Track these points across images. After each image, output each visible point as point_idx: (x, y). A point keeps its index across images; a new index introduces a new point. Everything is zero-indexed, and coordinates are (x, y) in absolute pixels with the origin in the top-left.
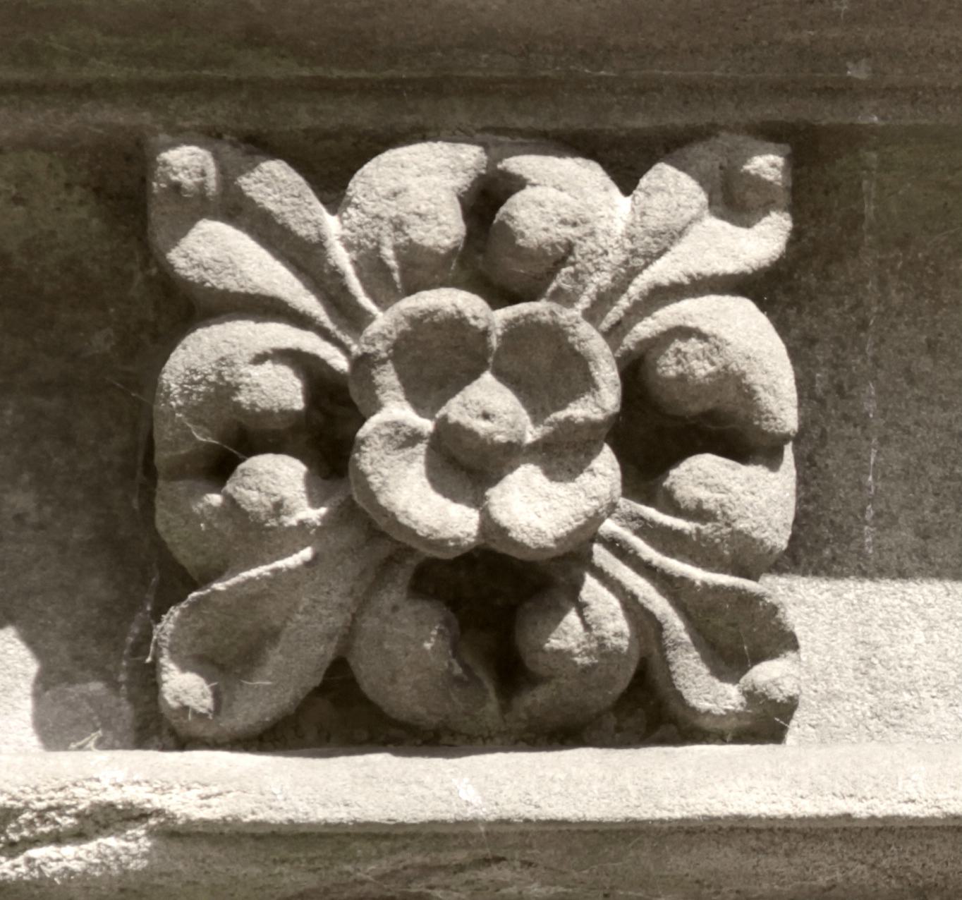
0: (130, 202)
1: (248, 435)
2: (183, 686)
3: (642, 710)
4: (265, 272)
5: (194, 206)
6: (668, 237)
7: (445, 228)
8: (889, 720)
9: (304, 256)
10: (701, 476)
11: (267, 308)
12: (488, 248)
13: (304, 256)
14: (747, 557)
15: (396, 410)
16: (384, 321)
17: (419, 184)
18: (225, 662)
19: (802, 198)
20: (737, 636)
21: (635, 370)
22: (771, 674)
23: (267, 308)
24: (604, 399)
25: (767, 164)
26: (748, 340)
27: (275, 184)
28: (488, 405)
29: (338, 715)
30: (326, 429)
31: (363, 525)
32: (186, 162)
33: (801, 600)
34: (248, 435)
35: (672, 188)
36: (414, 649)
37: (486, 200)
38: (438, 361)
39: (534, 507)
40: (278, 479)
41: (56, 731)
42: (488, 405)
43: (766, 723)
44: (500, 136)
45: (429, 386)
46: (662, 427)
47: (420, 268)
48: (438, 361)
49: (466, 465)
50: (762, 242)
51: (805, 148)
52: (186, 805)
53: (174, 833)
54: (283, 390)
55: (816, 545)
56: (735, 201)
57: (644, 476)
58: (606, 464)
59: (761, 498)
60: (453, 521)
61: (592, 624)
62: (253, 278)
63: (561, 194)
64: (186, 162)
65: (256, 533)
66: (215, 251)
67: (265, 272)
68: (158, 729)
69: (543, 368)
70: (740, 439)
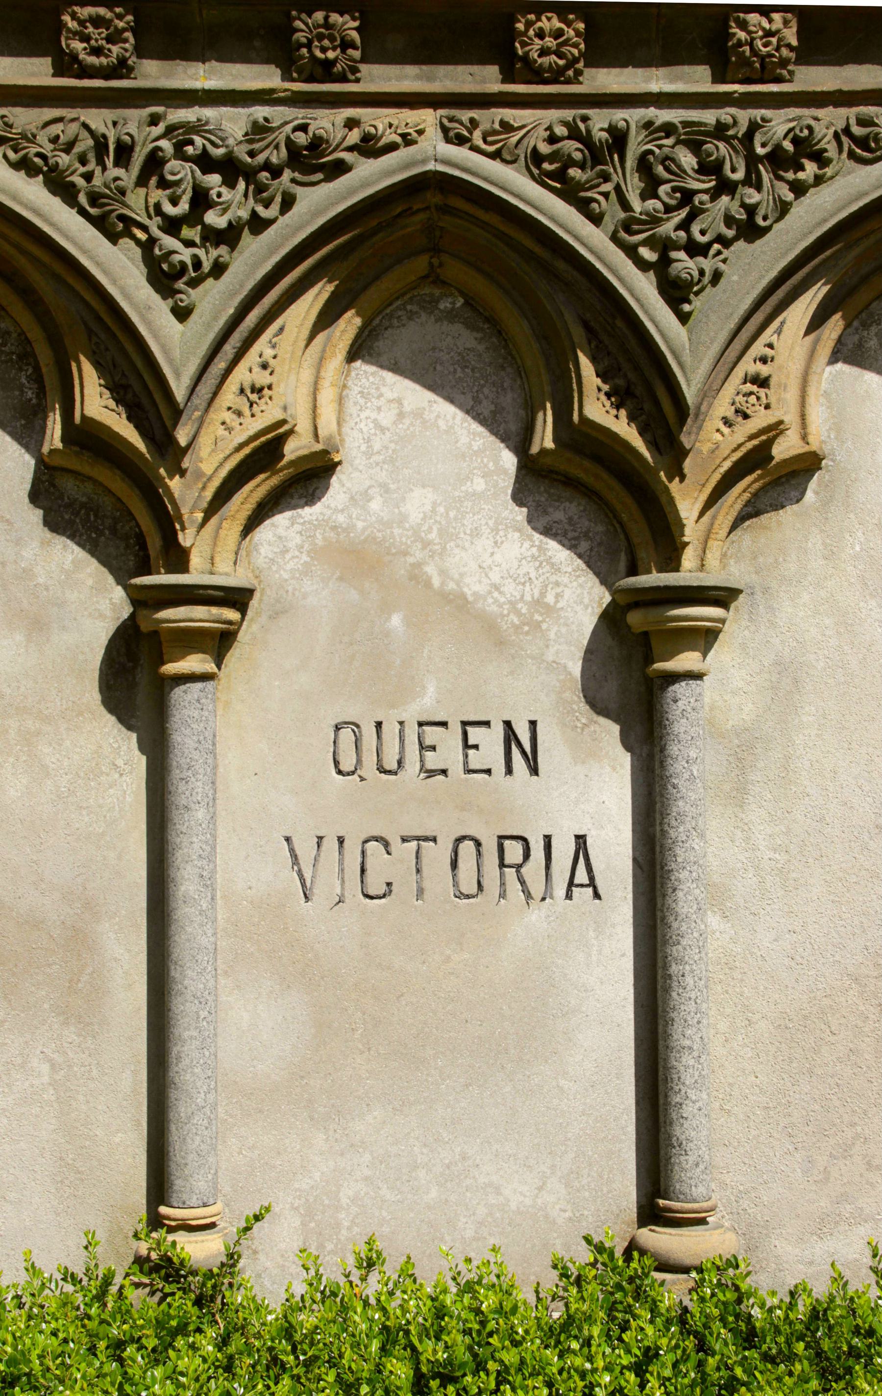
0: (291, 19)
1: (302, 45)
2: (295, 75)
3: (343, 79)
4: (303, 27)
5: (295, 19)
6: (346, 23)
7: (321, 21)
8: (372, 81)
9: (306, 24)
10: (350, 52)
11: (303, 31)
12: (327, 25)
13: (306, 24)
14: (355, 61)
15: (316, 43)
16: (315, 32)
17: (319, 16)
18: (299, 73)
19: (361, 18)
20: (355, 70)
21: (342, 39)
22: (358, 75)
23: (303, 31)
24: (338, 42)
25: (357, 14)
26: (355, 35)
27: (304, 16)
28: (326, 43)
29: (311, 79)
30: (309, 45)
31: (313, 56)
32: (294, 13)
33: (363, 67)
34: (302, 45)
35: (347, 17)
36: (319, 71)
37: (326, 18)
38: (320, 37)
39: (331, 55)
40: (304, 51)
41: (283, 80)
42: (326, 43)
43: (358, 81)
44: (328, 11)
45: (319, 42)
46: (346, 44)
47: (319, 26)
48: (320, 37)
49: (324, 50)
50: (356, 24)
51: (362, 13)
52: (294, 89)
53: (293, 92)
54: (304, 40)
55: (364, 60)
56: (354, 19)
57: (343, 51)
58: (339, 50)
59: (356, 54)
60: (322, 56)
61: (339, 67)
62: (303, 27)
63: (335, 18)
64: (294, 13)
65: (302, 57)
66: (298, 24)
67: (303, 27)
68: (293, 80)
69: (332, 39)
70: (355, 48)
